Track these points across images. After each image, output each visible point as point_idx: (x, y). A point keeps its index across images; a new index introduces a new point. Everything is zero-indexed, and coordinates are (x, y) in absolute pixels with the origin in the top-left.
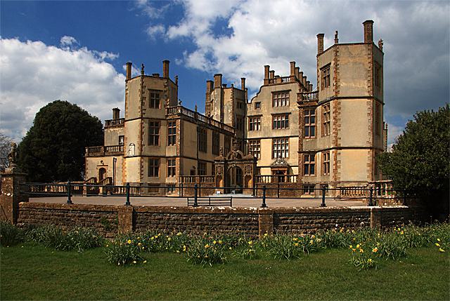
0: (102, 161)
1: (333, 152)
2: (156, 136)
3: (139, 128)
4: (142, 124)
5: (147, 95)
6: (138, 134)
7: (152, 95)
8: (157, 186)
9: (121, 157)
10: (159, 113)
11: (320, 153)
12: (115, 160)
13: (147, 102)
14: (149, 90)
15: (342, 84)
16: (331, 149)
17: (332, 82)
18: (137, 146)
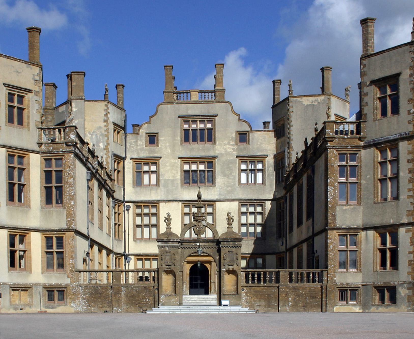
2: (20, 185)
8: (25, 289)
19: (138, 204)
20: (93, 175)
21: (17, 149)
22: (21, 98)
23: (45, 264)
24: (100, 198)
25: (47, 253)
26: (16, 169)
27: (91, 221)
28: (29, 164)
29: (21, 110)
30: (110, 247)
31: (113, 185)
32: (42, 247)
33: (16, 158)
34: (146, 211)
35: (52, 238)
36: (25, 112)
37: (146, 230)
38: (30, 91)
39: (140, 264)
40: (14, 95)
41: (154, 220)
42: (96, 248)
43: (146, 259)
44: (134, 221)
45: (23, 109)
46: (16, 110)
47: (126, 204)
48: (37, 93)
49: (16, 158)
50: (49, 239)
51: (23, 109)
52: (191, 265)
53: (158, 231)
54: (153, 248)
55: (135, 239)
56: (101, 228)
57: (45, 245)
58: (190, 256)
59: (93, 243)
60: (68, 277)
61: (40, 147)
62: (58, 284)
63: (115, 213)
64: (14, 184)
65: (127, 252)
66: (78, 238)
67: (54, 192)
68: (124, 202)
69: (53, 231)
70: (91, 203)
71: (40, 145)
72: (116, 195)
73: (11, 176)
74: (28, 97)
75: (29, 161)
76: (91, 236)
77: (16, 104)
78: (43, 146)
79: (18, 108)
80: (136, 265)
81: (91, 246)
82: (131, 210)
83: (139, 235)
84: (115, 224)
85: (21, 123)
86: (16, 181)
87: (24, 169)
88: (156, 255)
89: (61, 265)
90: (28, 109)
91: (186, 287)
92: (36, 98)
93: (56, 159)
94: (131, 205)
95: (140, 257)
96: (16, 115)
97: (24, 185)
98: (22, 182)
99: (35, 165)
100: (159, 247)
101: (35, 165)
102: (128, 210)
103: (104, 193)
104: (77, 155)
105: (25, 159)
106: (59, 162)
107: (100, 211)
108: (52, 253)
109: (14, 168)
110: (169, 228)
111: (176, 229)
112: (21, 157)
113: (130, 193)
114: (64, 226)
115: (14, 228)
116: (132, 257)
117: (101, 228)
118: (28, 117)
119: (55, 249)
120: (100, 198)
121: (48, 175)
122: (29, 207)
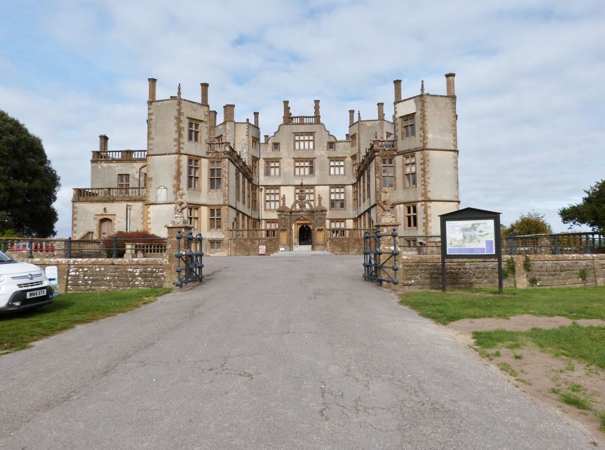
0: (105, 209)
1: (422, 205)
3: (175, 167)
4: (179, 162)
5: (185, 124)
6: (174, 174)
7: (190, 125)
9: (140, 204)
10: (199, 149)
11: (402, 206)
12: (128, 208)
13: (185, 134)
14: (189, 118)
15: (430, 135)
16: (419, 201)
17: (418, 132)
18: (171, 189)
19: (267, 187)
20: (239, 170)
21: (194, 156)
22: (197, 126)
23: (209, 226)
24: (244, 184)
25: (211, 219)
26: (193, 168)
27: (238, 199)
28: (201, 165)
29: (197, 133)
30: (249, 214)
31: (252, 176)
32: (208, 216)
33: (193, 162)
34: (272, 191)
35: (214, 210)
36: (199, 134)
37: (273, 204)
38: (202, 121)
39: (268, 225)
40: (193, 123)
41: (277, 198)
42: (241, 215)
43: (272, 222)
44: (265, 198)
45: (198, 132)
46: (193, 134)
47: (260, 187)
48: (206, 122)
49: (193, 162)
50: (212, 211)
51: (198, 132)
52: (300, 226)
53: (280, 205)
54: (275, 216)
55: (265, 210)
56: (244, 203)
57: (209, 213)
58: (297, 220)
59: (238, 212)
60: (223, 234)
61: (208, 154)
62: (217, 239)
63: (253, 193)
64: (192, 177)
65: (260, 218)
66: (231, 210)
67: (215, 182)
68: (258, 186)
69: (215, 205)
70: (238, 187)
71: (208, 153)
72: (253, 182)
73: (190, 172)
74: (201, 124)
75: (201, 163)
76: (238, 209)
77: (194, 129)
78: (210, 155)
79: (195, 131)
80: (266, 226)
81: (238, 214)
82: (263, 190)
83: (268, 207)
84: (253, 200)
85: (196, 140)
86: (193, 175)
87: (198, 168)
88: (277, 219)
89: (219, 227)
90: (201, 131)
91: (295, 240)
92: (205, 125)
93: (217, 162)
94: (263, 188)
95: (268, 221)
96: (194, 136)
97: (197, 178)
98: (197, 176)
99: (204, 164)
100: (279, 215)
101: (204, 164)
102: (261, 191)
103: (246, 180)
104: (230, 160)
105: (199, 162)
106: (219, 164)
107: (244, 192)
108: (214, 219)
109: (192, 167)
110: (284, 204)
111: (289, 204)
112: (196, 161)
113: (262, 180)
114: (221, 202)
115: (191, 204)
116: (263, 221)
117: (244, 203)
118: (201, 137)
119: (216, 217)
120: (244, 184)
121: (212, 171)
122: (200, 191)
